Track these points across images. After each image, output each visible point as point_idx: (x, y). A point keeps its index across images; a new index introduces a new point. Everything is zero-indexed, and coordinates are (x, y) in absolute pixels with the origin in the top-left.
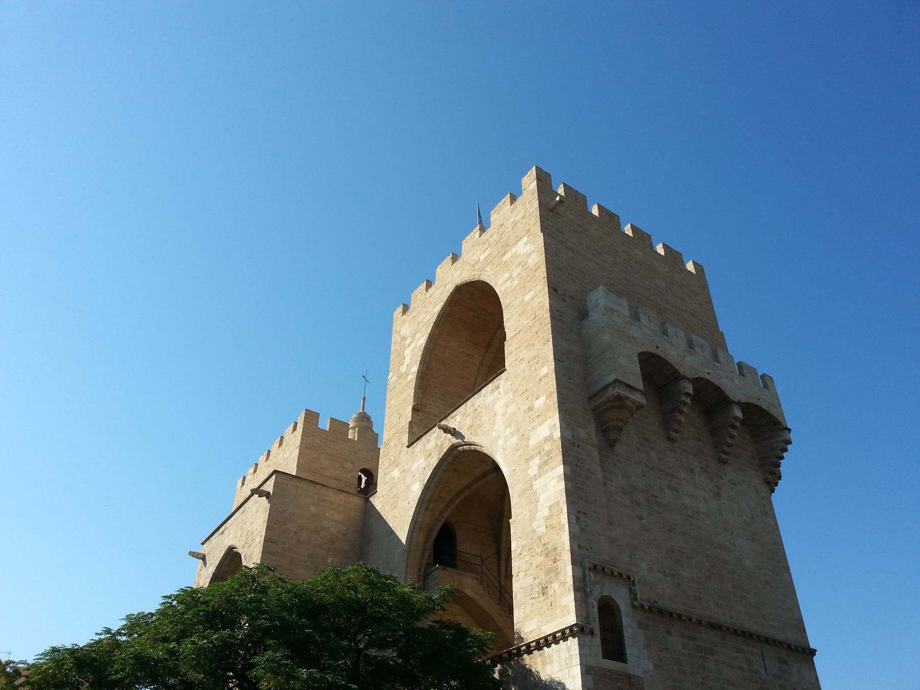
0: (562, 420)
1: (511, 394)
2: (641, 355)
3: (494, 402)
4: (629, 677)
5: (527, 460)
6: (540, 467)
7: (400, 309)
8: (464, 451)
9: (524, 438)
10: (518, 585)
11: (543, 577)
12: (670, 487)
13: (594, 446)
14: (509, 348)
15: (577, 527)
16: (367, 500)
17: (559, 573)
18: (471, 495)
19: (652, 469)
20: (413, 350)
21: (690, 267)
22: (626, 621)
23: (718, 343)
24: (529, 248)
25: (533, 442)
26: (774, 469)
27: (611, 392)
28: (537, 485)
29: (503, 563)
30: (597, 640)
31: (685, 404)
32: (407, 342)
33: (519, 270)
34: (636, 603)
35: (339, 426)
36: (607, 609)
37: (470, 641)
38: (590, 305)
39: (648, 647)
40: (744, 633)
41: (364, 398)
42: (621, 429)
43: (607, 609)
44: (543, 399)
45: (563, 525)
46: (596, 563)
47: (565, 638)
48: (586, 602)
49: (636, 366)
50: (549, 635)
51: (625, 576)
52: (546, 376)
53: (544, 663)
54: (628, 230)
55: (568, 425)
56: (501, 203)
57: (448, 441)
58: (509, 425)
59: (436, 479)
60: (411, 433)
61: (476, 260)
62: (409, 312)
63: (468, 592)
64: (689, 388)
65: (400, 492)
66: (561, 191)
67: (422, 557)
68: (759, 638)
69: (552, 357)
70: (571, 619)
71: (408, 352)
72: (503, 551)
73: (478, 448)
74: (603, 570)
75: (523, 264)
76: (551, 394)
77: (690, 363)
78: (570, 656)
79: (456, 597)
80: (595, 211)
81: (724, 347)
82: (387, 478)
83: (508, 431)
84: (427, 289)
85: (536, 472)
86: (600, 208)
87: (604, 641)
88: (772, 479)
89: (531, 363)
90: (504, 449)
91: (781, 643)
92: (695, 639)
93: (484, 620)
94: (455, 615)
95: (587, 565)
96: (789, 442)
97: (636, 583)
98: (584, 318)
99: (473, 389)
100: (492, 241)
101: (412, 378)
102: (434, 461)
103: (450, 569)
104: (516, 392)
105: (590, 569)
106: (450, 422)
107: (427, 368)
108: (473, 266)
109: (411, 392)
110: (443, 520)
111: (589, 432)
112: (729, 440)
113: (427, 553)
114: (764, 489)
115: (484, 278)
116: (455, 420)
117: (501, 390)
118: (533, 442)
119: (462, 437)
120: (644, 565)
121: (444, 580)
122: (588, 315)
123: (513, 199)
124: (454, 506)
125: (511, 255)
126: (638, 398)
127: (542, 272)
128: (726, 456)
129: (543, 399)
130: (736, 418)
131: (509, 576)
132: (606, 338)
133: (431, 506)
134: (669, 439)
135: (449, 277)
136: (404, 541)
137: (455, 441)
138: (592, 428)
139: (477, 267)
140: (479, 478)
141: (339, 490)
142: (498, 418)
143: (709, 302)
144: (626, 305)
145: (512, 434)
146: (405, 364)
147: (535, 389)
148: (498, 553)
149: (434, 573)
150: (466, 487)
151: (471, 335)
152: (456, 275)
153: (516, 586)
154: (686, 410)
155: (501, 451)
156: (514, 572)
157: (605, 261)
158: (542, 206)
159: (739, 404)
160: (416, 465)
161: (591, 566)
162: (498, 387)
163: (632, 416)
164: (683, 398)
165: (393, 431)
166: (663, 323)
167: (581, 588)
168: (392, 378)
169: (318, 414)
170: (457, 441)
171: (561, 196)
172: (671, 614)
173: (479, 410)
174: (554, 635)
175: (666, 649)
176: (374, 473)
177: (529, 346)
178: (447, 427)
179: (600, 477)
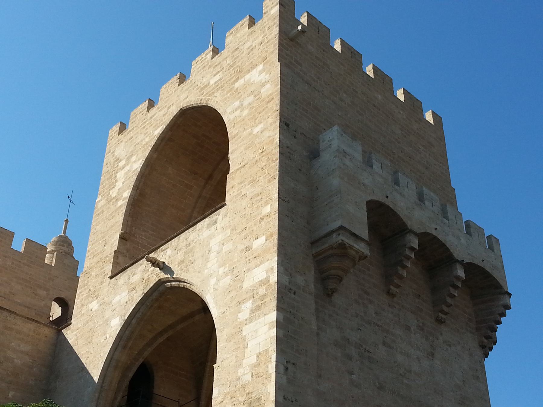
0: (280, 263)
1: (228, 231)
2: (369, 203)
3: (211, 237)
5: (239, 303)
6: (252, 312)
7: (116, 128)
8: (172, 288)
9: (238, 279)
15: (285, 378)
16: (59, 332)
20: (126, 173)
21: (429, 117)
23: (448, 198)
24: (264, 77)
25: (246, 285)
27: (336, 239)
28: (246, 330)
31: (409, 258)
32: (121, 164)
35: (35, 249)
38: (322, 145)
41: (67, 221)
42: (340, 279)
44: (262, 240)
45: (270, 375)
52: (268, 215)
54: (369, 71)
55: (286, 270)
56: (238, 25)
57: (155, 275)
58: (223, 264)
59: (139, 315)
61: (204, 83)
62: (126, 132)
64: (415, 243)
65: (97, 325)
66: (304, 20)
67: (115, 398)
69: (276, 195)
71: (120, 175)
72: (203, 397)
75: (256, 94)
76: (272, 235)
77: (418, 217)
80: (337, 46)
81: (454, 204)
82: (84, 310)
83: (221, 270)
85: (247, 316)
86: (343, 43)
89: (254, 200)
99: (188, 222)
100: (225, 64)
101: (122, 203)
102: (138, 296)
106: (161, 255)
107: (140, 194)
108: (202, 89)
109: (120, 219)
110: (141, 360)
111: (307, 279)
113: (121, 394)
115: (212, 104)
116: (167, 254)
118: (246, 285)
119: (171, 272)
123: (252, 22)
124: (155, 345)
126: (362, 248)
127: (275, 104)
128: (444, 316)
129: (262, 240)
132: (336, 182)
133: (130, 344)
134: (389, 293)
135: (175, 98)
136: (96, 379)
137: (163, 276)
138: (311, 276)
140: (184, 319)
141: (29, 319)
142: (213, 255)
144: (360, 148)
145: (226, 274)
146: (117, 188)
147: (255, 228)
150: (171, 327)
151: (190, 165)
152: (183, 97)
154: (409, 265)
155: (212, 291)
157: (342, 100)
159: (461, 262)
160: (117, 298)
162: (216, 222)
164: (408, 252)
165: (95, 260)
166: (396, 172)
168: (100, 201)
169: (13, 234)
170: (165, 276)
171: (303, 26)
173: (193, 245)
176: (69, 303)
177: (254, 182)
178: (156, 260)
179: (314, 327)
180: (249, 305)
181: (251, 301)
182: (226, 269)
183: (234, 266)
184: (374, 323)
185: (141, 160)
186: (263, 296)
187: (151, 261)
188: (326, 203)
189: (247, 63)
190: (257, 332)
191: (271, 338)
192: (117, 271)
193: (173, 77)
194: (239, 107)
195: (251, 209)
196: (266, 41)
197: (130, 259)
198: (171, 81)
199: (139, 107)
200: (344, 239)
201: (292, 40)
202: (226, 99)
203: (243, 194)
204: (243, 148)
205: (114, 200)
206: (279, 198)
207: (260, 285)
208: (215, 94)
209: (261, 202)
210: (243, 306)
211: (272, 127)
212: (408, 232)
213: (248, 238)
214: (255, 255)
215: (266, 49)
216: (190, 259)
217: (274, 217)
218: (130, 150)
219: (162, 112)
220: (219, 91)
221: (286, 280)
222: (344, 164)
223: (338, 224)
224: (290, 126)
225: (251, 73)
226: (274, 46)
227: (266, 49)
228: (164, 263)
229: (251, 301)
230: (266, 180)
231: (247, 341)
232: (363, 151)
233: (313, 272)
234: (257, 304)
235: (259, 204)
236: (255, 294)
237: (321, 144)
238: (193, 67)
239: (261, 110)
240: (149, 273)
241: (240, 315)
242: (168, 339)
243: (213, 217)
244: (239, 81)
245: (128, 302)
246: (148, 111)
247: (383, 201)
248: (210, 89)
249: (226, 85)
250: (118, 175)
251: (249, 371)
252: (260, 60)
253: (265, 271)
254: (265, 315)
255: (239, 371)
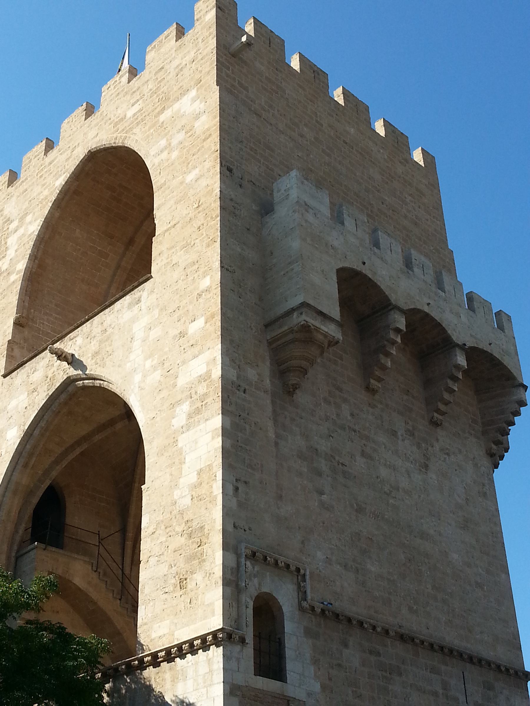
1: (156, 312)
2: (340, 271)
3: (134, 320)
4: (288, 701)
5: (173, 406)
6: (190, 416)
8: (84, 387)
9: (171, 375)
10: (147, 575)
11: (182, 565)
12: (363, 454)
13: (266, 392)
14: (159, 246)
15: (234, 500)
17: (204, 561)
18: (91, 453)
19: (343, 428)
20: (20, 238)
21: (417, 156)
22: (289, 627)
23: (444, 265)
24: (199, 106)
25: (182, 381)
26: (500, 437)
27: (297, 319)
28: (183, 440)
29: (129, 544)
30: (249, 651)
31: (394, 343)
32: (13, 226)
33: (181, 136)
34: (304, 604)
36: (266, 613)
37: (76, 650)
38: (277, 196)
39: (315, 662)
40: (442, 648)
42: (305, 372)
43: (266, 613)
44: (200, 322)
45: (216, 497)
46: (255, 548)
47: (205, 647)
48: (238, 601)
49: (332, 287)
50: (185, 643)
51: (293, 568)
52: (208, 290)
53: (174, 680)
54: (338, 96)
55: (233, 361)
56: (162, 37)
57: (62, 371)
58: (151, 356)
59: (43, 424)
60: (10, 357)
62: (17, 183)
63: (78, 581)
64: (401, 323)
66: (249, 28)
67: (16, 531)
68: (461, 655)
69: (217, 264)
70: (215, 622)
71: (12, 241)
73: (105, 384)
74: (265, 559)
75: (189, 130)
76: (213, 316)
77: (405, 290)
78: (211, 671)
79: (60, 587)
80: (295, 63)
81: (451, 269)
83: (148, 364)
84: (46, 152)
85: (184, 422)
86: (302, 59)
87: (258, 652)
88: (497, 450)
89: (188, 271)
90: (141, 388)
91: (489, 663)
92: (378, 654)
93: (95, 619)
94: (57, 613)
95: (244, 551)
96: (523, 403)
97: (307, 577)
98: (267, 214)
99: (104, 301)
101: (16, 278)
102: (41, 399)
103: (54, 549)
104: (163, 309)
105: (248, 556)
106: (68, 345)
107: (40, 266)
108: (116, 124)
109: (13, 299)
110: (48, 483)
111: (261, 373)
112: (446, 396)
114: (485, 462)
116: (75, 343)
117: (143, 305)
118: (182, 381)
119: (83, 367)
120: (320, 555)
121: (44, 564)
122: (273, 210)
123: (181, 33)
124: (65, 463)
125: (170, 116)
126: (332, 330)
127: (214, 143)
128: (440, 417)
129: (200, 322)
130: (458, 367)
131: (136, 562)
132: (296, 244)
135: (80, 138)
137: (72, 372)
138: (266, 368)
139: (120, 127)
142: (137, 344)
143: (438, 206)
144: (327, 200)
145: (154, 368)
146: (8, 258)
147: (191, 307)
148: (124, 530)
149: (32, 553)
151: (103, 225)
152: (92, 134)
153: (144, 574)
155: (136, 390)
156: (143, 557)
157: (302, 136)
158: (222, 48)
159: (463, 347)
160: (14, 403)
161: (249, 552)
162: (139, 301)
163: (322, 353)
164: (392, 335)
166: (375, 231)
167: (232, 582)
170: (76, 372)
171: (249, 36)
172: (349, 620)
173: (110, 330)
174: (191, 643)
175: (339, 665)
177: (187, 246)
178: (63, 352)
179: (271, 434)
180: (185, 407)
181: (188, 403)
182: (155, 362)
183: (165, 357)
184: (349, 428)
185: (39, 221)
186: (203, 395)
187: (56, 354)
188: (282, 273)
189: (175, 89)
190: (197, 443)
191: (216, 450)
192: (12, 368)
193: (76, 107)
194: (166, 148)
195: (185, 281)
196: (200, 57)
197: (29, 351)
198: (75, 113)
199: (34, 150)
200: (308, 319)
201: (234, 55)
202: (148, 136)
203: (174, 262)
204: (172, 202)
205: (5, 274)
206: (222, 267)
207: (199, 382)
208: (134, 131)
209: (198, 273)
210: (178, 409)
211: (211, 173)
212: (393, 309)
213: (182, 321)
214: (191, 343)
215: (200, 69)
216: (108, 349)
217: (215, 291)
218: (24, 207)
219: (64, 156)
220: (140, 126)
221: (233, 374)
222: (306, 221)
223: (300, 299)
224: (234, 171)
225: (180, 101)
226: (211, 64)
227: (200, 69)
228: (73, 355)
229: (188, 403)
230: (204, 244)
231: (184, 454)
232: (331, 202)
233: (268, 363)
234: (196, 406)
235: (196, 275)
236: (193, 393)
237: (275, 194)
238: (103, 94)
239: (195, 150)
240: (55, 369)
241: (174, 422)
242: (82, 454)
243: (136, 293)
244: (166, 112)
245: (28, 408)
246: (46, 154)
247: (359, 269)
248: (126, 124)
249: (148, 118)
250: (10, 241)
251: (187, 493)
252: (192, 83)
253: (206, 363)
254: (207, 420)
255: (175, 493)
